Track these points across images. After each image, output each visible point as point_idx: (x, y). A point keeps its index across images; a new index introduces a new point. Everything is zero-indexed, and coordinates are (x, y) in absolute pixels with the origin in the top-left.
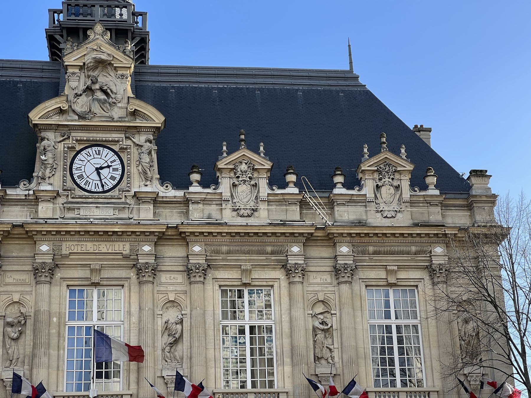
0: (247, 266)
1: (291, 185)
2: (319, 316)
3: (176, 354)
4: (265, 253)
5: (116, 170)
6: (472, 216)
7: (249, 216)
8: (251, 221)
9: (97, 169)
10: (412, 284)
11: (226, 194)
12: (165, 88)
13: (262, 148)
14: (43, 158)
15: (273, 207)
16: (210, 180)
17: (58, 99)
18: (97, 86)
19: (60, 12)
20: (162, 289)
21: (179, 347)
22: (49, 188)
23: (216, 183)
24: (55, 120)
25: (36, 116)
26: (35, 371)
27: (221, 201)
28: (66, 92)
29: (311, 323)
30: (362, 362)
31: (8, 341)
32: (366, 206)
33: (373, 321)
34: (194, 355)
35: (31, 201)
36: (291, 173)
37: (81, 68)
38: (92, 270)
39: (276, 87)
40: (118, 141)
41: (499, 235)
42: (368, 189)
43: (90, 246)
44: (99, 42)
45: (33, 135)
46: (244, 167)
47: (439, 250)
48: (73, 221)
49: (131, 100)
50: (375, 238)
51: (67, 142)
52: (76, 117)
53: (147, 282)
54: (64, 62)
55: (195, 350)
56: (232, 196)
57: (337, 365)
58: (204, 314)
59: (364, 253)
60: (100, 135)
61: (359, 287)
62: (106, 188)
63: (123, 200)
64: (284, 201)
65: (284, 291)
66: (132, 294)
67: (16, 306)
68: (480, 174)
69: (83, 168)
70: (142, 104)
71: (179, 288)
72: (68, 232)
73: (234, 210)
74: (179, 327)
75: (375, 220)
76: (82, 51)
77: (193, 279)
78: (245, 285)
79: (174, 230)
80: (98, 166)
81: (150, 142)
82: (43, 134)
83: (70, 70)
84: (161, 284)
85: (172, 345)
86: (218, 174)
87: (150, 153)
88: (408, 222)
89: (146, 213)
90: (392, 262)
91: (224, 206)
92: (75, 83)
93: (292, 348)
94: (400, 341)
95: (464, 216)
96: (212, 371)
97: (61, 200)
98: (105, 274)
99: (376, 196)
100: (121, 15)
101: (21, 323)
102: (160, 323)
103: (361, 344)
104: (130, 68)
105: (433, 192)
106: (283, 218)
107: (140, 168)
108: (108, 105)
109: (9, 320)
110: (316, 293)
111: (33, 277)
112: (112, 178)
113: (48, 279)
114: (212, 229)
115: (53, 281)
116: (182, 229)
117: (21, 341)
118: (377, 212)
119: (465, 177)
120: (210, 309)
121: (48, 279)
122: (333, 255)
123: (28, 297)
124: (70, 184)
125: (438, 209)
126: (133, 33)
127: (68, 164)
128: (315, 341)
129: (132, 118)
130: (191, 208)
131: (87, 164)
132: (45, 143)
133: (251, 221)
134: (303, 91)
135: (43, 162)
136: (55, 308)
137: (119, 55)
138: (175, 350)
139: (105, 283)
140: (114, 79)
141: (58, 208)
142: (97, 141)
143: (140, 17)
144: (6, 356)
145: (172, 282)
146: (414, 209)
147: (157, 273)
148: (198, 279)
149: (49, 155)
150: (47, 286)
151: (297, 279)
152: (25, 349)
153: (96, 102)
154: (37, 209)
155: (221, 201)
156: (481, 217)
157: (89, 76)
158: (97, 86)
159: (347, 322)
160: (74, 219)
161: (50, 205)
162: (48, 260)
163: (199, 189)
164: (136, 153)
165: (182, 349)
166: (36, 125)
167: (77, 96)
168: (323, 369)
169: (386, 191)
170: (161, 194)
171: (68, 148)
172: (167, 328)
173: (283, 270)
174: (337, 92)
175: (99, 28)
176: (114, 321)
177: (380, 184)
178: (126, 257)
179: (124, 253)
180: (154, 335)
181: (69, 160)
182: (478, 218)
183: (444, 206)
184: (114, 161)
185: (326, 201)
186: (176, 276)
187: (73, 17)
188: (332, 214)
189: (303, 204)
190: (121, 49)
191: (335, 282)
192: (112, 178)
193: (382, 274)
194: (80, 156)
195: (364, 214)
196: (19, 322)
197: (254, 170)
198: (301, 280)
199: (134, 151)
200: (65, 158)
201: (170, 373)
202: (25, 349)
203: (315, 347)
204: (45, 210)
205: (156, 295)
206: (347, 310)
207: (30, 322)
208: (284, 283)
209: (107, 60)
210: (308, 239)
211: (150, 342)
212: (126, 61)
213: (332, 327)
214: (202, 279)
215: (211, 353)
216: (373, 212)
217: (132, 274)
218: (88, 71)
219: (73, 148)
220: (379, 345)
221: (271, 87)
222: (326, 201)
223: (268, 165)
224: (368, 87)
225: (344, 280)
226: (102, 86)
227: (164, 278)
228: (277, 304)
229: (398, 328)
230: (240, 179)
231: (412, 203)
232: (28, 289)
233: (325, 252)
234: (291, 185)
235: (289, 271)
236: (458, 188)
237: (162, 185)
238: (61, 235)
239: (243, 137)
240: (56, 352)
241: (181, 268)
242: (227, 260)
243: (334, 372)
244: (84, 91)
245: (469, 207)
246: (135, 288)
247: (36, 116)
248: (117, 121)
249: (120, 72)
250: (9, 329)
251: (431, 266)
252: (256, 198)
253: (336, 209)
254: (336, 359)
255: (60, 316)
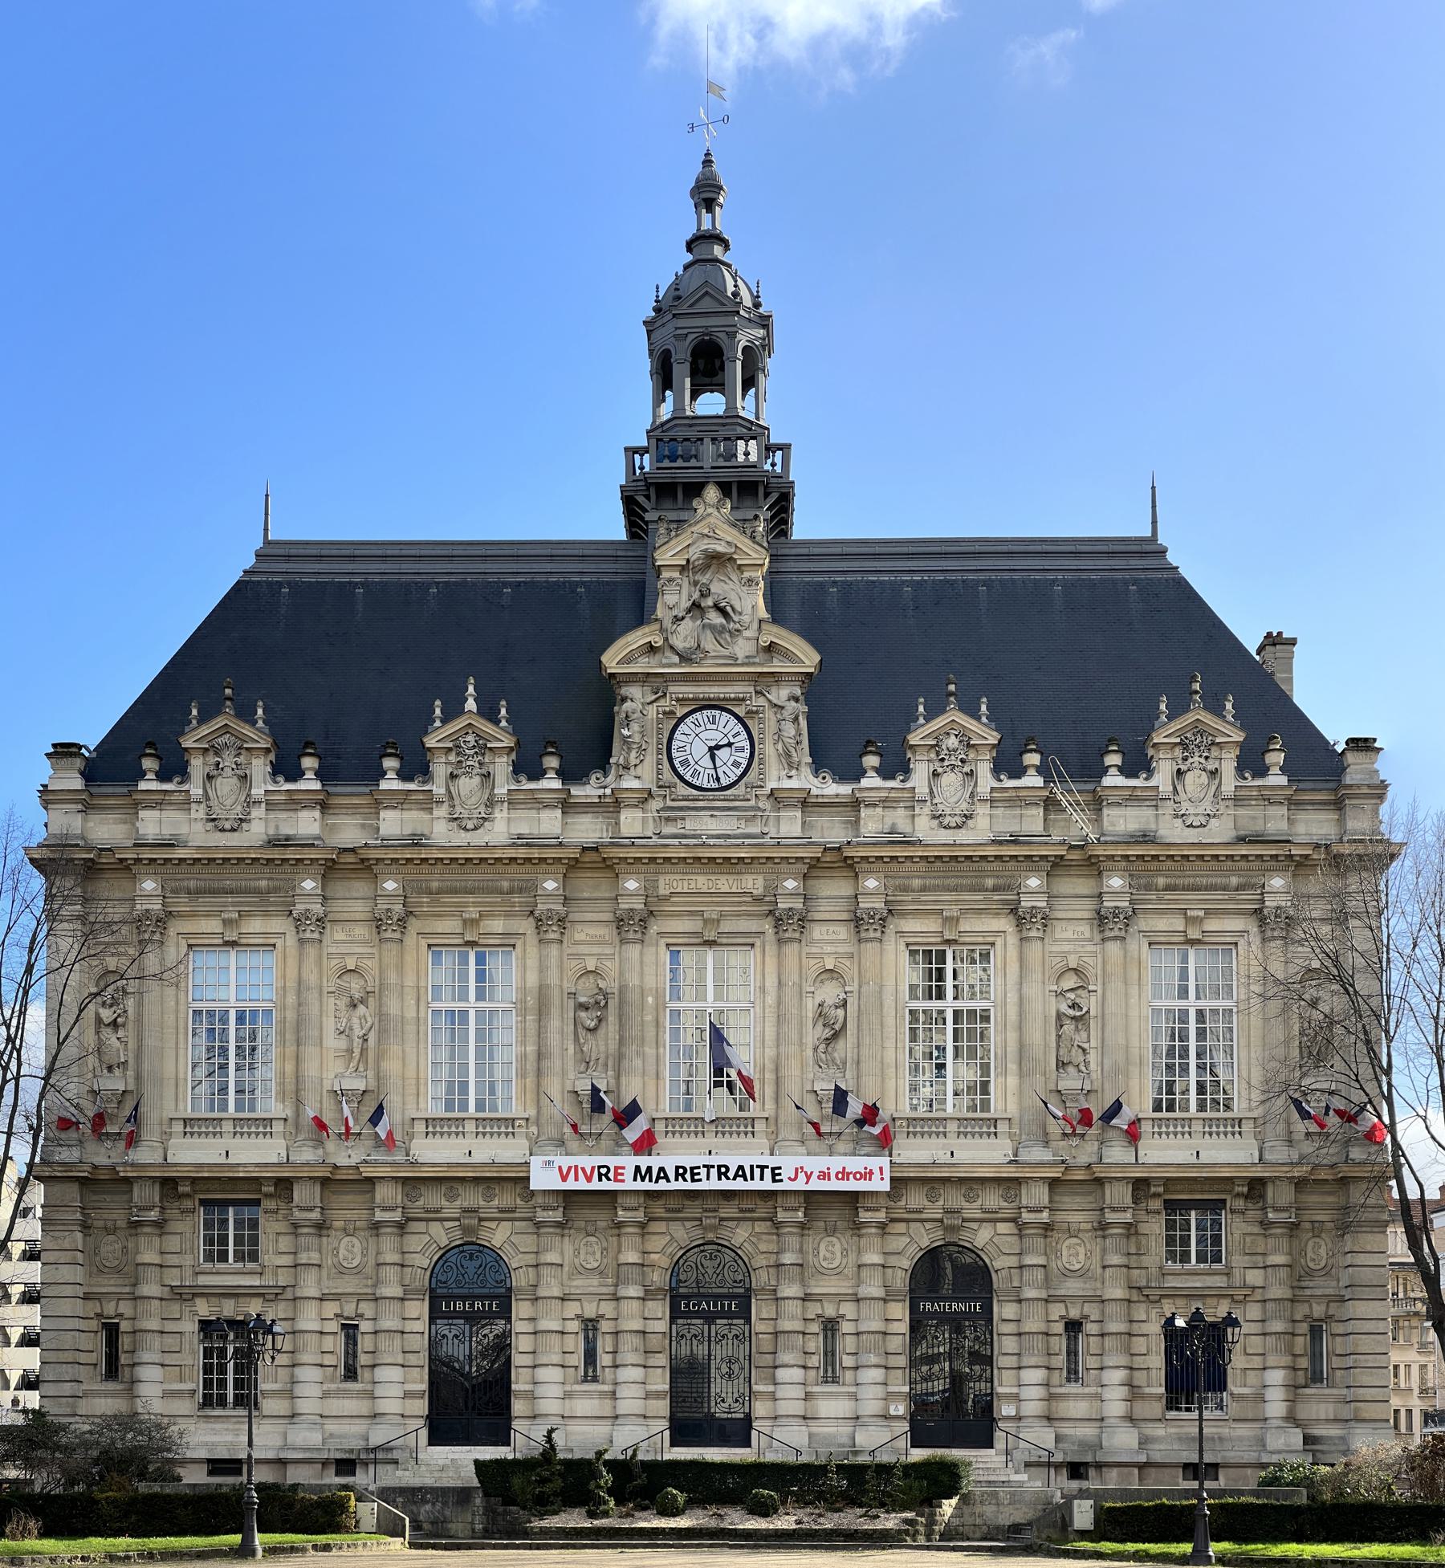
0: (952, 911)
1: (1032, 771)
2: (1068, 995)
3: (836, 1055)
4: (982, 889)
5: (742, 749)
6: (1341, 821)
7: (958, 827)
8: (962, 836)
9: (711, 749)
10: (1229, 940)
11: (922, 790)
12: (821, 585)
13: (984, 708)
14: (625, 732)
15: (999, 812)
16: (896, 766)
17: (646, 629)
18: (710, 602)
19: (642, 451)
20: (814, 950)
21: (840, 1044)
22: (635, 784)
23: (906, 771)
24: (641, 666)
25: (612, 660)
26: (623, 1080)
27: (912, 802)
28: (660, 613)
29: (1054, 1006)
30: (1134, 1070)
31: (582, 1033)
32: (1156, 806)
33: (1157, 1003)
34: (862, 1058)
35: (607, 805)
36: (1031, 751)
37: (683, 569)
38: (705, 921)
39: (1016, 576)
40: (743, 699)
41: (1380, 856)
42: (1162, 778)
43: (702, 882)
44: (712, 520)
45: (607, 691)
46: (952, 742)
47: (1277, 882)
48: (676, 841)
49: (764, 626)
50: (1169, 863)
51: (662, 702)
52: (676, 659)
53: (791, 940)
54: (654, 560)
55: (864, 1051)
56: (931, 792)
57: (1094, 1076)
58: (880, 992)
59: (1148, 888)
60: (715, 689)
61: (1137, 946)
62: (724, 782)
63: (752, 803)
64: (1017, 800)
65: (1013, 953)
66: (767, 959)
67: (591, 977)
68: (1362, 745)
69: (688, 748)
70: (783, 632)
71: (842, 949)
72: (667, 860)
73: (934, 817)
74: (840, 1012)
75: (1172, 831)
76: (684, 539)
77: (863, 935)
78: (948, 942)
79: (835, 853)
80: (713, 744)
81: (797, 700)
82: (625, 691)
83: (665, 575)
84: (813, 942)
85: (829, 1041)
86: (909, 755)
87: (796, 719)
88: (1228, 835)
89: (790, 824)
90: (1195, 904)
91: (917, 809)
92: (673, 597)
93: (1022, 1046)
94: (1201, 1034)
95: (1327, 820)
96: (891, 1084)
97: (655, 804)
98: (726, 927)
99: (1175, 788)
100: (747, 454)
101: (599, 1004)
102: (810, 1005)
103: (1135, 1042)
104: (762, 565)
105: (1277, 779)
106: (1015, 828)
107: (780, 746)
108: (727, 636)
109: (582, 999)
110: (1065, 955)
111: (615, 932)
112: (736, 764)
113: (639, 936)
114: (898, 851)
115: (647, 937)
116: (848, 852)
117: (601, 1032)
118: (1176, 816)
119: (1339, 749)
120: (889, 983)
121: (639, 936)
122: (1096, 892)
123: (608, 963)
124: (668, 775)
125: (1283, 810)
126: (766, 487)
127: (665, 741)
128: (1059, 1037)
129: (767, 656)
130: (863, 815)
131: (696, 740)
132: (628, 705)
133: (962, 836)
134: (1065, 583)
135: (625, 740)
136: (650, 982)
137: (744, 543)
138: (834, 1049)
139: (724, 941)
140: (737, 587)
141: (651, 820)
142: (709, 699)
143: (779, 454)
144: (579, 1056)
145: (829, 938)
146: (1241, 812)
147: (807, 925)
148: (872, 934)
149: (635, 727)
150: (638, 946)
151: (1033, 933)
152: (607, 1045)
153: (708, 632)
154: (618, 818)
155: (912, 802)
156: (1357, 823)
157: (696, 583)
158: (710, 602)
159: (1112, 1006)
160: (675, 836)
161: (638, 813)
162: (638, 904)
163: (877, 782)
164: (774, 719)
165: (844, 1048)
166: (612, 675)
167: (678, 620)
168: (1070, 1082)
169: (1195, 780)
170: (814, 792)
171: (664, 713)
172: (821, 1014)
173: (1011, 917)
174: (1126, 582)
175: (712, 493)
176: (739, 1001)
177: (1183, 768)
178: (758, 900)
179: (755, 892)
180: (801, 1024)
181: (666, 734)
182: (1351, 824)
183: (1293, 803)
184: (738, 734)
185: (1089, 797)
186: (836, 929)
187: (666, 463)
188: (1098, 821)
189: (1050, 804)
190: (748, 532)
191: (1098, 937)
192: (736, 764)
193: (1178, 924)
194: (682, 727)
195: (1152, 819)
196: (597, 1003)
197: (969, 745)
198: (1040, 934)
199: (770, 715)
200: (659, 732)
201: (825, 1086)
202: (607, 1045)
203: (1058, 1046)
204: (631, 822)
205: (804, 960)
206: (1115, 985)
207: (613, 1004)
208: (1012, 940)
209: (725, 554)
210: (1055, 865)
211: (795, 1037)
212: (756, 555)
213: (1088, 1012)
214: (878, 934)
215: (890, 1055)
216: (1167, 817)
217: (767, 926)
218: (695, 573)
219: (672, 713)
220: (1164, 1043)
221: (1006, 576)
222: (1089, 797)
223: (993, 738)
224: (1184, 572)
225: (1112, 934)
226: (717, 602)
227: (817, 932)
228: (1000, 974)
229: (1200, 1014)
230: (946, 763)
231: (1237, 800)
232: (608, 950)
233: (1083, 885)
234: (1032, 771)
235: (1021, 918)
236: (1326, 769)
237: (816, 773)
238: (656, 863)
239: (952, 688)
240: (654, 1051)
241: (845, 916)
242: (920, 902)
243: (1087, 1087)
244: (689, 611)
245: (1338, 805)
246: (771, 949)
247: (612, 660)
248: (742, 665)
249: (746, 575)
250: (583, 1014)
251: (1261, 910)
252: (972, 795)
253: (1105, 811)
254: (1093, 1066)
255: (658, 994)
